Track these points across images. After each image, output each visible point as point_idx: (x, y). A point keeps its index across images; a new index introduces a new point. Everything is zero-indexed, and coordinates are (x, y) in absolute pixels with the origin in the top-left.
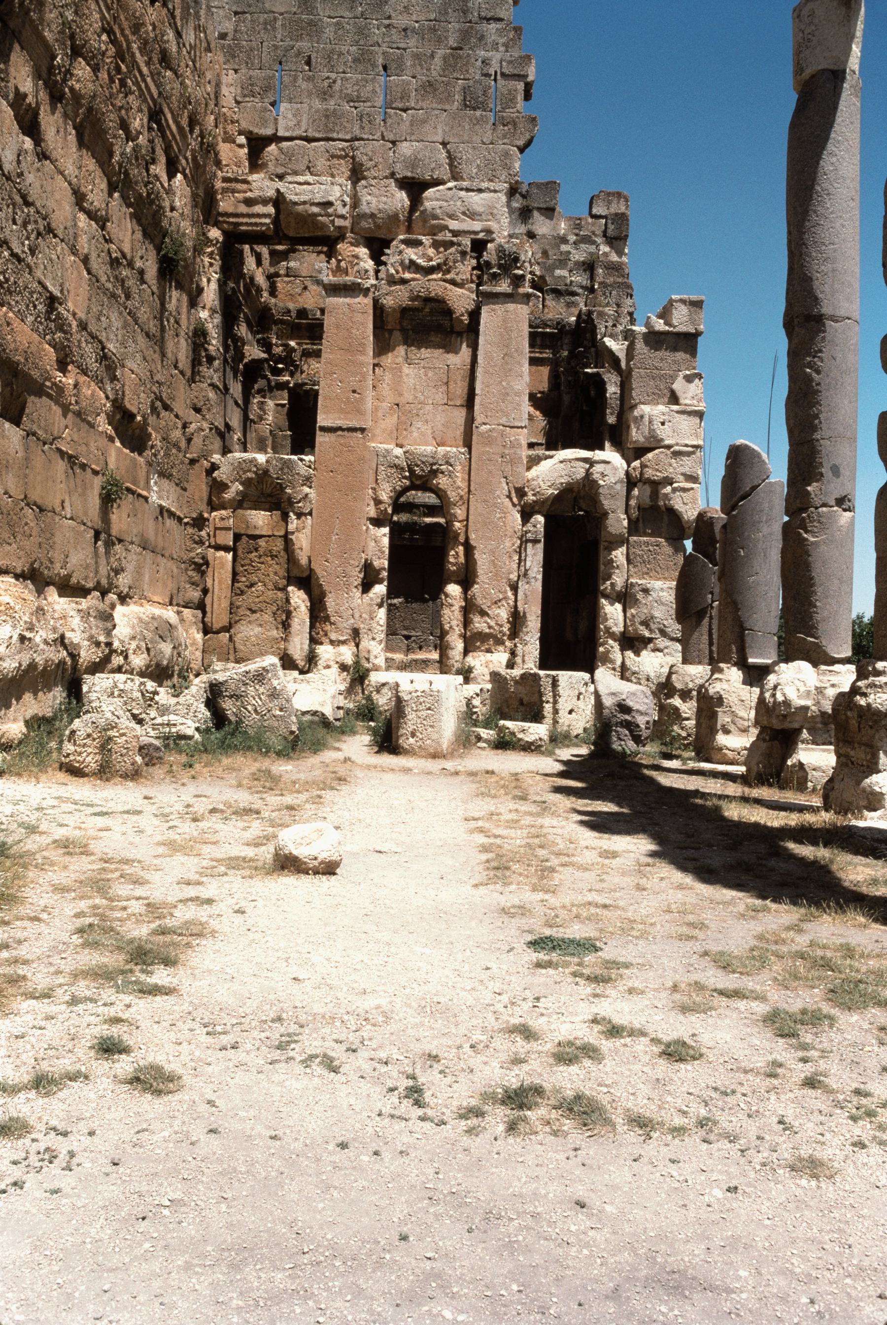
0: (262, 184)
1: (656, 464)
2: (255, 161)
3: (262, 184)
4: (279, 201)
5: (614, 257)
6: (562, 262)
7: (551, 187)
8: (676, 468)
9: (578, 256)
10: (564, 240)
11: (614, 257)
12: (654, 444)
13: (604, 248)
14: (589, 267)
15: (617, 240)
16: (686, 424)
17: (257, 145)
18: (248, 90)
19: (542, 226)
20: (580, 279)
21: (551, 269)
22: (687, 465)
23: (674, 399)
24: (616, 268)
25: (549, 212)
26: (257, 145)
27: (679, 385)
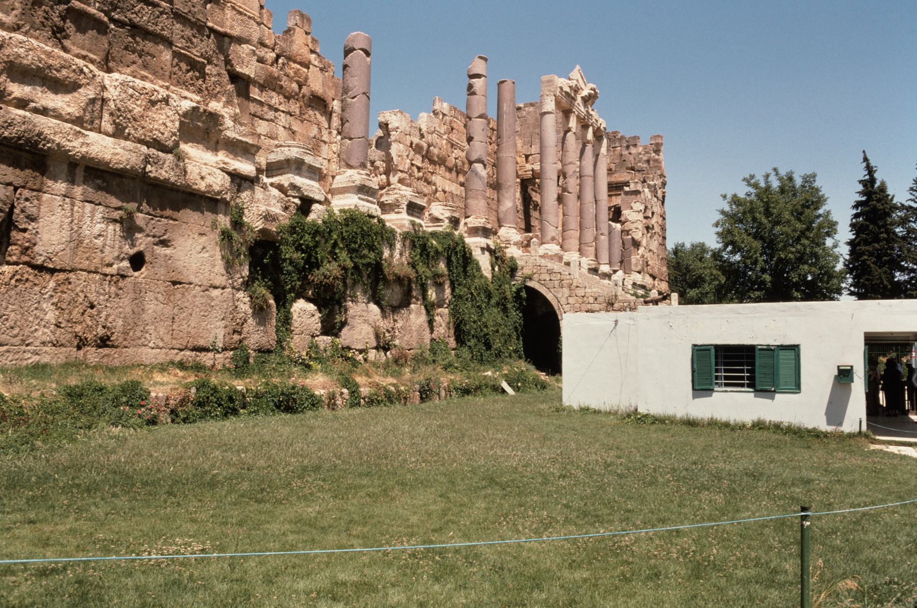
0: (529, 167)
1: (627, 226)
2: (527, 161)
3: (529, 167)
4: (533, 170)
5: (657, 157)
6: (640, 161)
7: (636, 138)
8: (632, 226)
9: (645, 158)
10: (640, 154)
11: (657, 157)
12: (626, 221)
13: (653, 154)
14: (648, 161)
15: (657, 151)
16: (635, 214)
17: (527, 157)
18: (524, 144)
19: (633, 150)
20: (645, 165)
21: (636, 164)
22: (635, 225)
23: (632, 208)
24: (656, 161)
25: (635, 145)
26: (527, 157)
27: (632, 204)
